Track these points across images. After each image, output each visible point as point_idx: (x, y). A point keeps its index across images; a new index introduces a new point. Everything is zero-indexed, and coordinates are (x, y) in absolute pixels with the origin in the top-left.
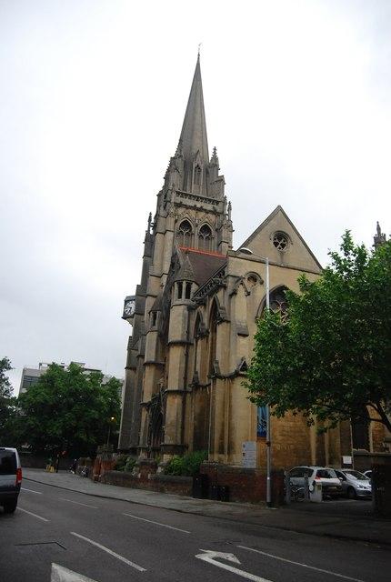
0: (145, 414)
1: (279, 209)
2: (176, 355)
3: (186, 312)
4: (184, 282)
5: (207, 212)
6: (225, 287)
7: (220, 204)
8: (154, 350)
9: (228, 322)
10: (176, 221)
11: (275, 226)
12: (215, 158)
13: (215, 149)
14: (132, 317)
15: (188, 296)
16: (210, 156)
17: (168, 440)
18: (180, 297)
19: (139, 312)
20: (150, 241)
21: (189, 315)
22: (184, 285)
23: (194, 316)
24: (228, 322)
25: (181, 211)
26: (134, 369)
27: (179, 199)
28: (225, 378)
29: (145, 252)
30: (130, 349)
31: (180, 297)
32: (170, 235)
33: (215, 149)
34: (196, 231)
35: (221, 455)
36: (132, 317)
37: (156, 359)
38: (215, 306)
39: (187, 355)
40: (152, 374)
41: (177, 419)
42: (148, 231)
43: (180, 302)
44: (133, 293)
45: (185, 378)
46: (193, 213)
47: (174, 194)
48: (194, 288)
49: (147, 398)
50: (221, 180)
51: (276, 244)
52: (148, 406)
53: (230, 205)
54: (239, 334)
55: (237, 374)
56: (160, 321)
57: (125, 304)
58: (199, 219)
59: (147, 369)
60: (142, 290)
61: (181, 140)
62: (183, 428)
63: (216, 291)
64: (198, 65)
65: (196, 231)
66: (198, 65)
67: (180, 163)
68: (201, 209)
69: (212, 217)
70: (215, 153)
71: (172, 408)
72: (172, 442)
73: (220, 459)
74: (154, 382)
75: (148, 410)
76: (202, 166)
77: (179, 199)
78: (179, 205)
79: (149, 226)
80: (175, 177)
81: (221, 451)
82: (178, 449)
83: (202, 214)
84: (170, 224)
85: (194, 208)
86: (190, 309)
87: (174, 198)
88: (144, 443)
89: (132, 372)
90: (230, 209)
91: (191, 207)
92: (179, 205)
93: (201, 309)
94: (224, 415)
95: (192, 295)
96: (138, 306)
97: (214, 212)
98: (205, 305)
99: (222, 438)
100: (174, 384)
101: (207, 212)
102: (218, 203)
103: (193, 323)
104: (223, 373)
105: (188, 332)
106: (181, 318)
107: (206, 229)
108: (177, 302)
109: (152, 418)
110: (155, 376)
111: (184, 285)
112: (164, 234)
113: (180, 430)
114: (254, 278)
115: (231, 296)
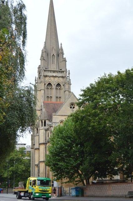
3: (45, 132)
10: (45, 84)
15: (45, 125)
16: (60, 45)
21: (46, 133)
22: (43, 121)
25: (47, 79)
34: (54, 87)
46: (52, 78)
50: (65, 60)
53: (69, 72)
58: (54, 81)
59: (36, 151)
65: (54, 87)
70: (61, 46)
75: (37, 167)
83: (56, 79)
86: (46, 130)
90: (69, 74)
92: (46, 76)
101: (59, 77)
107: (59, 85)
108: (41, 128)
111: (43, 121)
113: (45, 175)
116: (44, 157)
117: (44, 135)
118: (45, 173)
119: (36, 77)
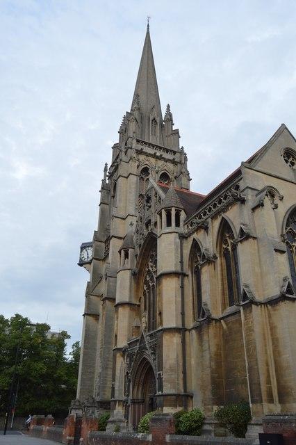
0: (121, 363)
1: (283, 125)
2: (169, 288)
3: (178, 240)
4: (173, 209)
5: (166, 160)
6: (243, 201)
7: (177, 155)
8: (128, 290)
9: (255, 238)
11: (283, 144)
12: (169, 114)
13: (168, 106)
14: (90, 263)
15: (178, 225)
17: (168, 389)
18: (169, 224)
19: (101, 257)
20: (109, 191)
22: (173, 212)
23: (188, 245)
24: (255, 238)
25: (142, 157)
26: (96, 316)
27: (139, 147)
28: (261, 304)
29: (102, 198)
30: (88, 294)
31: (169, 224)
32: (133, 179)
33: (168, 106)
35: (271, 406)
36: (90, 263)
37: (130, 297)
38: (225, 227)
39: (182, 287)
40: (127, 315)
41: (177, 361)
42: (104, 181)
43: (169, 229)
44: (90, 239)
45: (183, 314)
46: (153, 160)
47: (134, 142)
48: (183, 215)
49: (122, 343)
50: (177, 132)
51: (287, 161)
52: (123, 351)
54: (276, 250)
55: (283, 298)
56: (132, 261)
57: (81, 252)
59: (120, 309)
60: (103, 237)
61: (137, 96)
62: (184, 373)
63: (225, 209)
64: (148, 33)
66: (148, 33)
67: (136, 113)
68: (160, 158)
69: (170, 166)
71: (171, 346)
72: (173, 391)
73: (270, 411)
74: (130, 324)
75: (123, 356)
76: (158, 121)
77: (139, 147)
78: (140, 152)
79: (105, 176)
80: (132, 127)
81: (271, 401)
82: (184, 398)
83: (161, 163)
84: (133, 168)
85: (154, 156)
86: (183, 237)
87: (135, 145)
88: (120, 394)
89: (90, 318)
91: (149, 155)
93: (200, 236)
94: (266, 350)
95: (182, 223)
96: (96, 252)
97: (173, 162)
98: (206, 229)
99: (269, 382)
100: (170, 319)
101: (166, 160)
102: (175, 153)
103: (187, 251)
104: (258, 298)
105: (182, 262)
106: (173, 246)
109: (129, 366)
110: (130, 317)
111: (173, 212)
112: (127, 178)
114: (271, 193)
115: (254, 209)
116: (177, 315)
117: (176, 249)
118: (181, 369)
119: (106, 164)
